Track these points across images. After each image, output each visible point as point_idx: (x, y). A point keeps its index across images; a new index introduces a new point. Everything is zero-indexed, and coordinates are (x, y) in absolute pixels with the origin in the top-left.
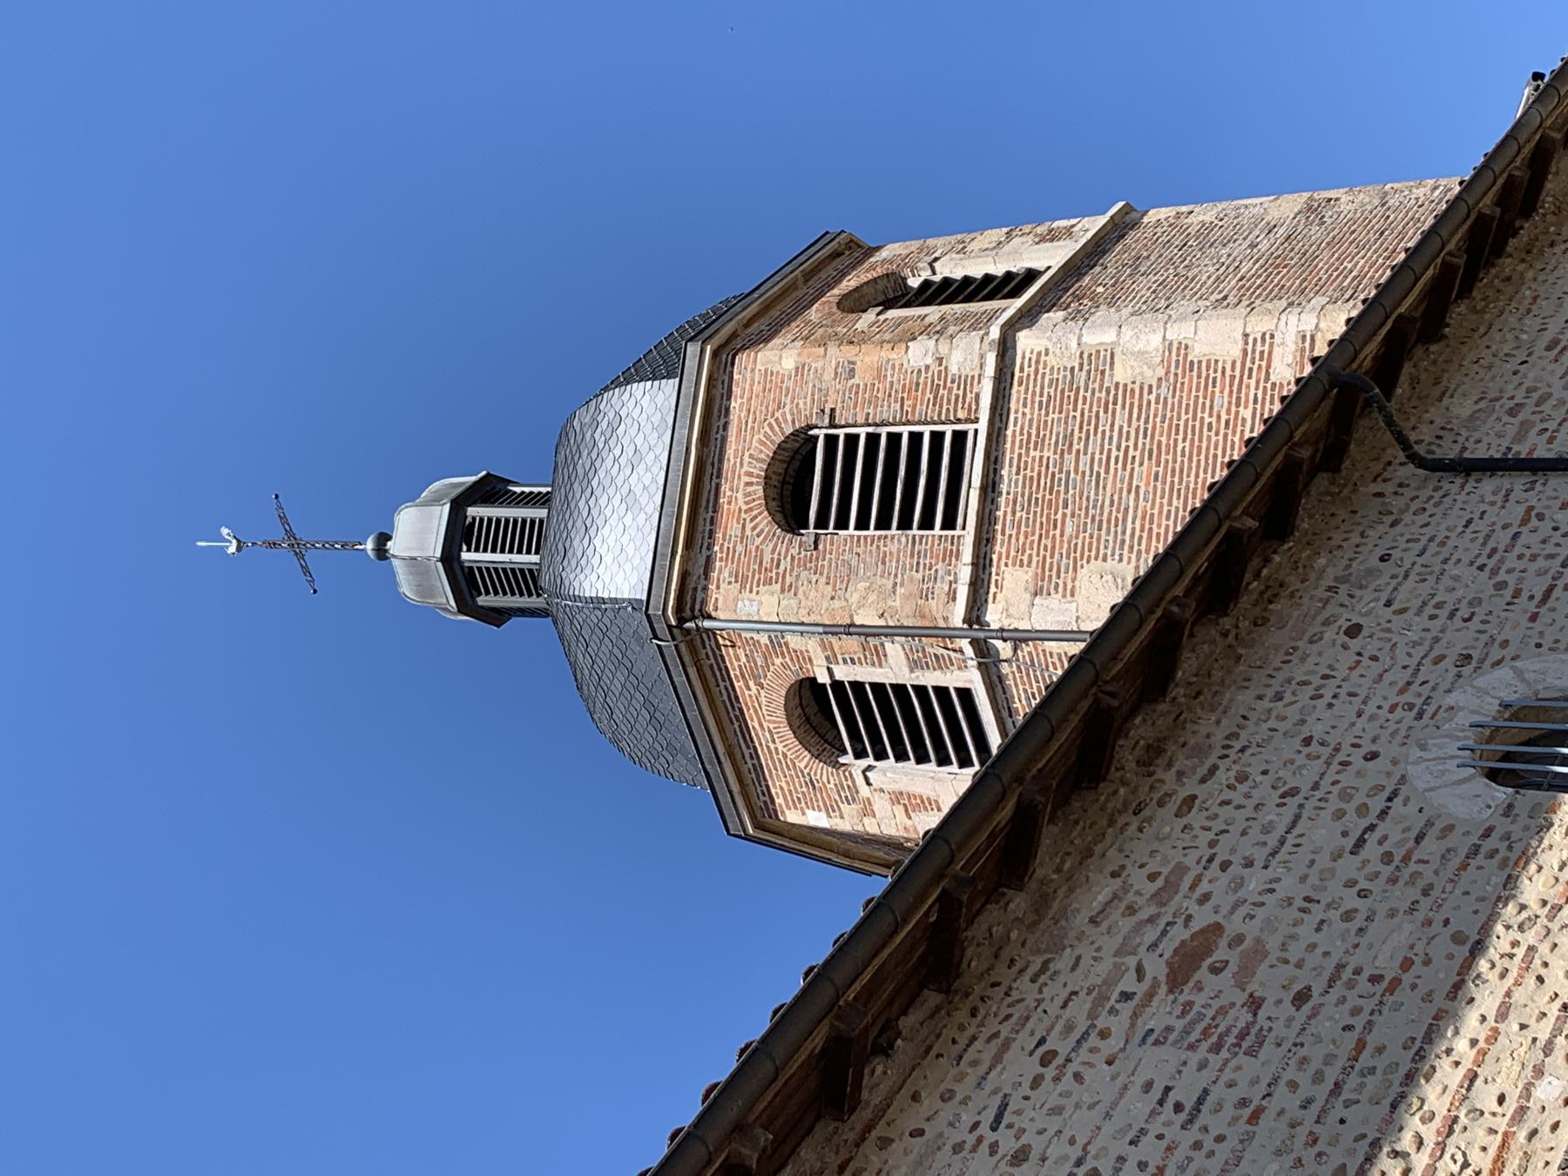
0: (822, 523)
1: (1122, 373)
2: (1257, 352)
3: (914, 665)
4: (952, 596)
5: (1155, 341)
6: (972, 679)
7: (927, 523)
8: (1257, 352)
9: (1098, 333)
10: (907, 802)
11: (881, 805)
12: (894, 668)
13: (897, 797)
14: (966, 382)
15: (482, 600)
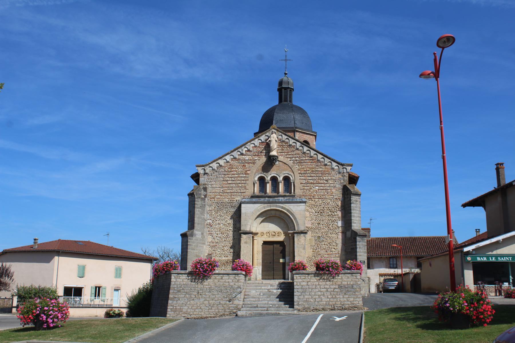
15: (283, 90)
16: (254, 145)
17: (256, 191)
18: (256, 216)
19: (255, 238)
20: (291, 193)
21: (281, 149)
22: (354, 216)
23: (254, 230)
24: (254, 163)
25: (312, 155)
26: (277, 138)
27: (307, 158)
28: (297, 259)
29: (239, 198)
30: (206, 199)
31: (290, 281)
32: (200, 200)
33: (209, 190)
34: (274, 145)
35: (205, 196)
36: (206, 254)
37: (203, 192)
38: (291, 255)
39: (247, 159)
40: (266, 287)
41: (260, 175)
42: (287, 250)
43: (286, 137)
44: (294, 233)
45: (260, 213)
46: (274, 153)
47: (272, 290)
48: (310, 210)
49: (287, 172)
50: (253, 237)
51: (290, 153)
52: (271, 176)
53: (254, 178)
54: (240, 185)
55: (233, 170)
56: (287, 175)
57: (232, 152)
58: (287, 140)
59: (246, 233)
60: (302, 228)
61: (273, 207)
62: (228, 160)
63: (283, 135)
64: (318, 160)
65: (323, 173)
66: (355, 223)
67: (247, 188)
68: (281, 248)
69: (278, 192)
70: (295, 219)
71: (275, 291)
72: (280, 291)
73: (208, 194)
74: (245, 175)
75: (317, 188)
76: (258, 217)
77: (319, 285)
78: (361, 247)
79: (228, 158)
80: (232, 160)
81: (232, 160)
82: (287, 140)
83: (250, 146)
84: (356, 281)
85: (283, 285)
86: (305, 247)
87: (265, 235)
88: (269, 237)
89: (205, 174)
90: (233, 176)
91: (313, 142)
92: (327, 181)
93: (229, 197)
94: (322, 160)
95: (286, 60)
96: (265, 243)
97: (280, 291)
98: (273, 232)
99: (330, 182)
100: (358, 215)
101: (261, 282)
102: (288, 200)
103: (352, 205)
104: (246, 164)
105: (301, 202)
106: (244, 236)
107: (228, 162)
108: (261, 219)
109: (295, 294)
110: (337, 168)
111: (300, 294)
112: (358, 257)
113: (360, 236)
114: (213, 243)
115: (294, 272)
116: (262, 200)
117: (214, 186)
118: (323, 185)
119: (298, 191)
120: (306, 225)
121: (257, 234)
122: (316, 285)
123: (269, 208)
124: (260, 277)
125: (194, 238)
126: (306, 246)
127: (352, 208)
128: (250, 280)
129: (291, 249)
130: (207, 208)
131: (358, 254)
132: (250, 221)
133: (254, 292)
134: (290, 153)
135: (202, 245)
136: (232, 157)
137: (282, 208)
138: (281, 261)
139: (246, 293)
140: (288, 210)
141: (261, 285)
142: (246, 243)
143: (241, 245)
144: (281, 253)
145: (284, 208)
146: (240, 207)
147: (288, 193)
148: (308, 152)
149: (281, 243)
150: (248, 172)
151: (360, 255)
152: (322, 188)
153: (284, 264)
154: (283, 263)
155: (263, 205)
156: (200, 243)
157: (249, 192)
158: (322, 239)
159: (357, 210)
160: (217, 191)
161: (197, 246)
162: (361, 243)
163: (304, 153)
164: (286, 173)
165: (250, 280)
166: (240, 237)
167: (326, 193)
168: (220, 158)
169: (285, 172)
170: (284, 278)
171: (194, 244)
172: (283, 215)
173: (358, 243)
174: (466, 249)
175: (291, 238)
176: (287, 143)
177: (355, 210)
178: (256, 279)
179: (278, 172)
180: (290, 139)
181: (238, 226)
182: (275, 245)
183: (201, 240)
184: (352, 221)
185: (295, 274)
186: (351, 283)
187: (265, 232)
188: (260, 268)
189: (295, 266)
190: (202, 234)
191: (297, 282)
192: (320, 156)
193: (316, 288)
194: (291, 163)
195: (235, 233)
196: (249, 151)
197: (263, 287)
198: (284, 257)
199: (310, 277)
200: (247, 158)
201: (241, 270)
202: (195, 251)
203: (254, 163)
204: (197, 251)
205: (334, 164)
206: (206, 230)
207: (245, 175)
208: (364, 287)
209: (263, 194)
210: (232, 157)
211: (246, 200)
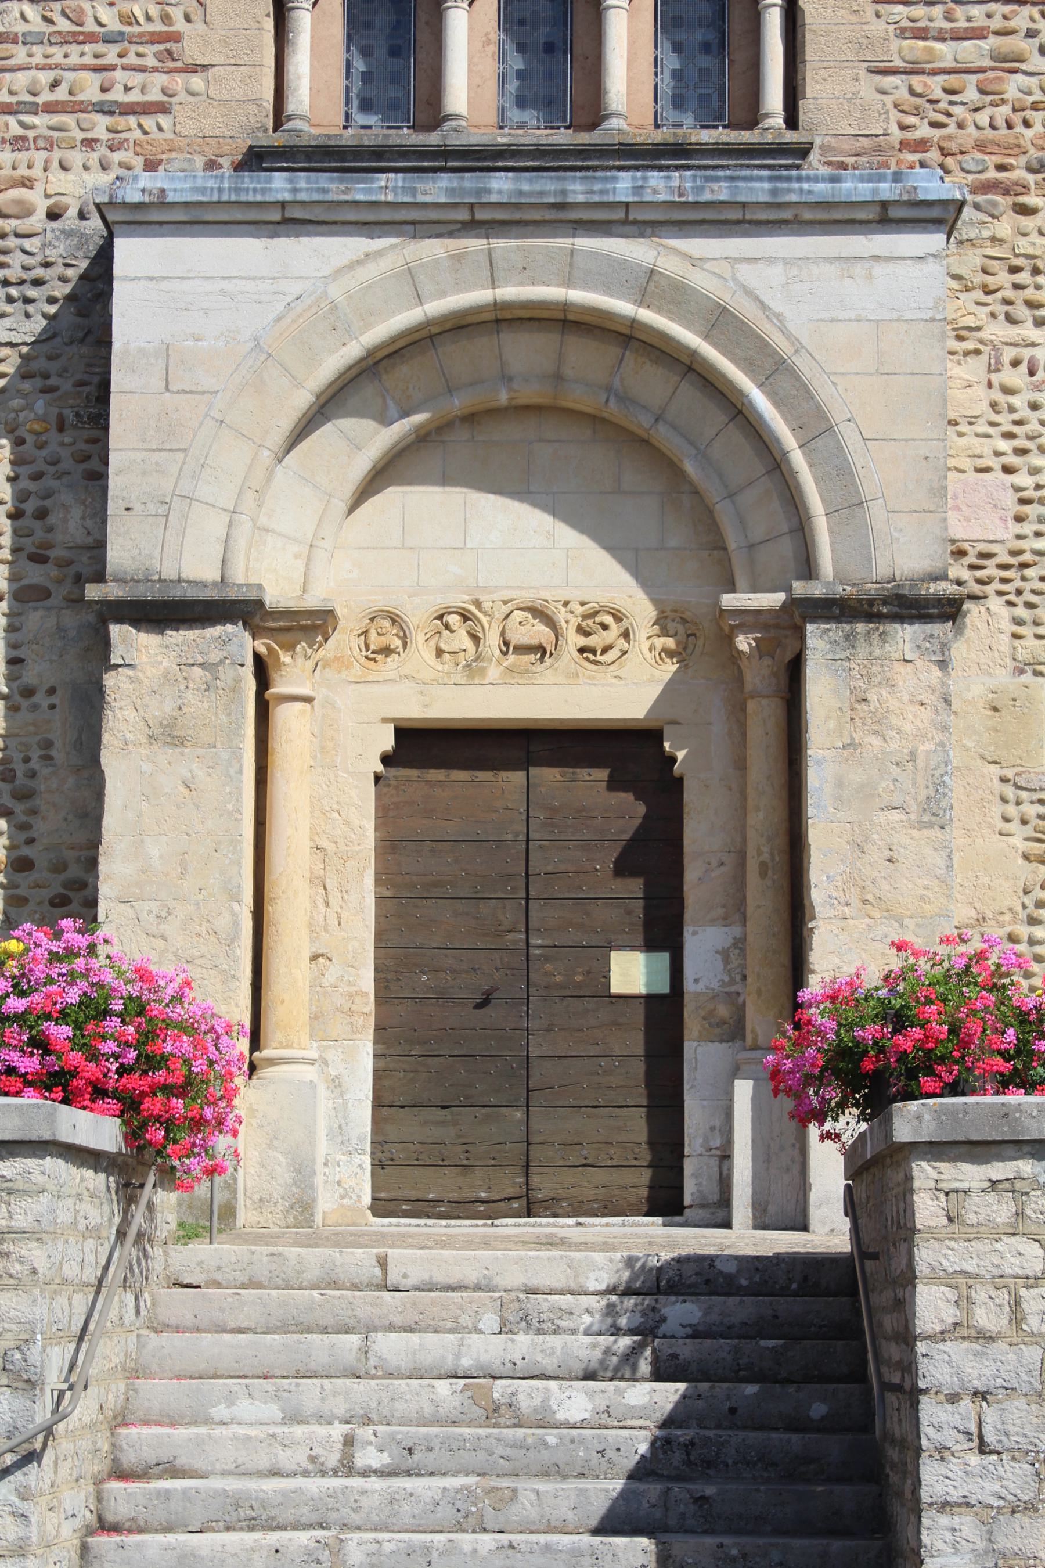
17: (301, 97)
18: (303, 399)
19: (294, 674)
20: (752, 118)
28: (846, 953)
29: (80, 183)
31: (744, 1239)
38: (762, 899)
40: (436, 1347)
42: (702, 832)
44: (803, 611)
45: (353, 351)
47: (528, 1395)
48: (997, 331)
60: (903, 554)
61: (533, 273)
67: (191, 51)
68: (627, 812)
69: (594, 114)
70: (816, 426)
71: (575, 1402)
72: (658, 1397)
76: (331, 403)
85: (681, 1312)
86: (940, 787)
87: (422, 651)
88: (473, 670)
96: (419, 746)
97: (658, 1397)
98: (526, 600)
101: (360, 1261)
105: (886, 217)
106: (142, 654)
108: (361, 441)
109: (935, 1479)
111: (1014, 1478)
115: (913, 1119)
116: (385, 187)
119: (846, 100)
120: (958, 530)
121: (313, 625)
123: (480, 296)
124: (347, 1176)
126: (956, 786)
128: (213, 1220)
129: (763, 816)
133: (253, 1410)
137: (649, 285)
138: (632, 972)
139: (141, 1442)
140: (720, 321)
141: (366, 1304)
142: (170, 735)
143: (112, 762)
144: (623, 868)
145: (674, 295)
146: (97, 281)
147: (711, 118)
149: (627, 752)
153: (664, 1012)
154: (650, 999)
155: (391, 253)
157: (222, 103)
165: (213, 1220)
166: (98, 654)
170: (666, 1202)
172: (650, 383)
175: (759, 676)
178: (302, 1208)
181: (70, 525)
182: (547, 776)
185: (937, 1150)
187: (417, 615)
188: (358, 1064)
189: (899, 1020)
191: (962, 1284)
195: (35, 619)
197: (390, 1346)
198: (663, 933)
201: (60, 1085)
209: (407, 137)
211: (179, 183)
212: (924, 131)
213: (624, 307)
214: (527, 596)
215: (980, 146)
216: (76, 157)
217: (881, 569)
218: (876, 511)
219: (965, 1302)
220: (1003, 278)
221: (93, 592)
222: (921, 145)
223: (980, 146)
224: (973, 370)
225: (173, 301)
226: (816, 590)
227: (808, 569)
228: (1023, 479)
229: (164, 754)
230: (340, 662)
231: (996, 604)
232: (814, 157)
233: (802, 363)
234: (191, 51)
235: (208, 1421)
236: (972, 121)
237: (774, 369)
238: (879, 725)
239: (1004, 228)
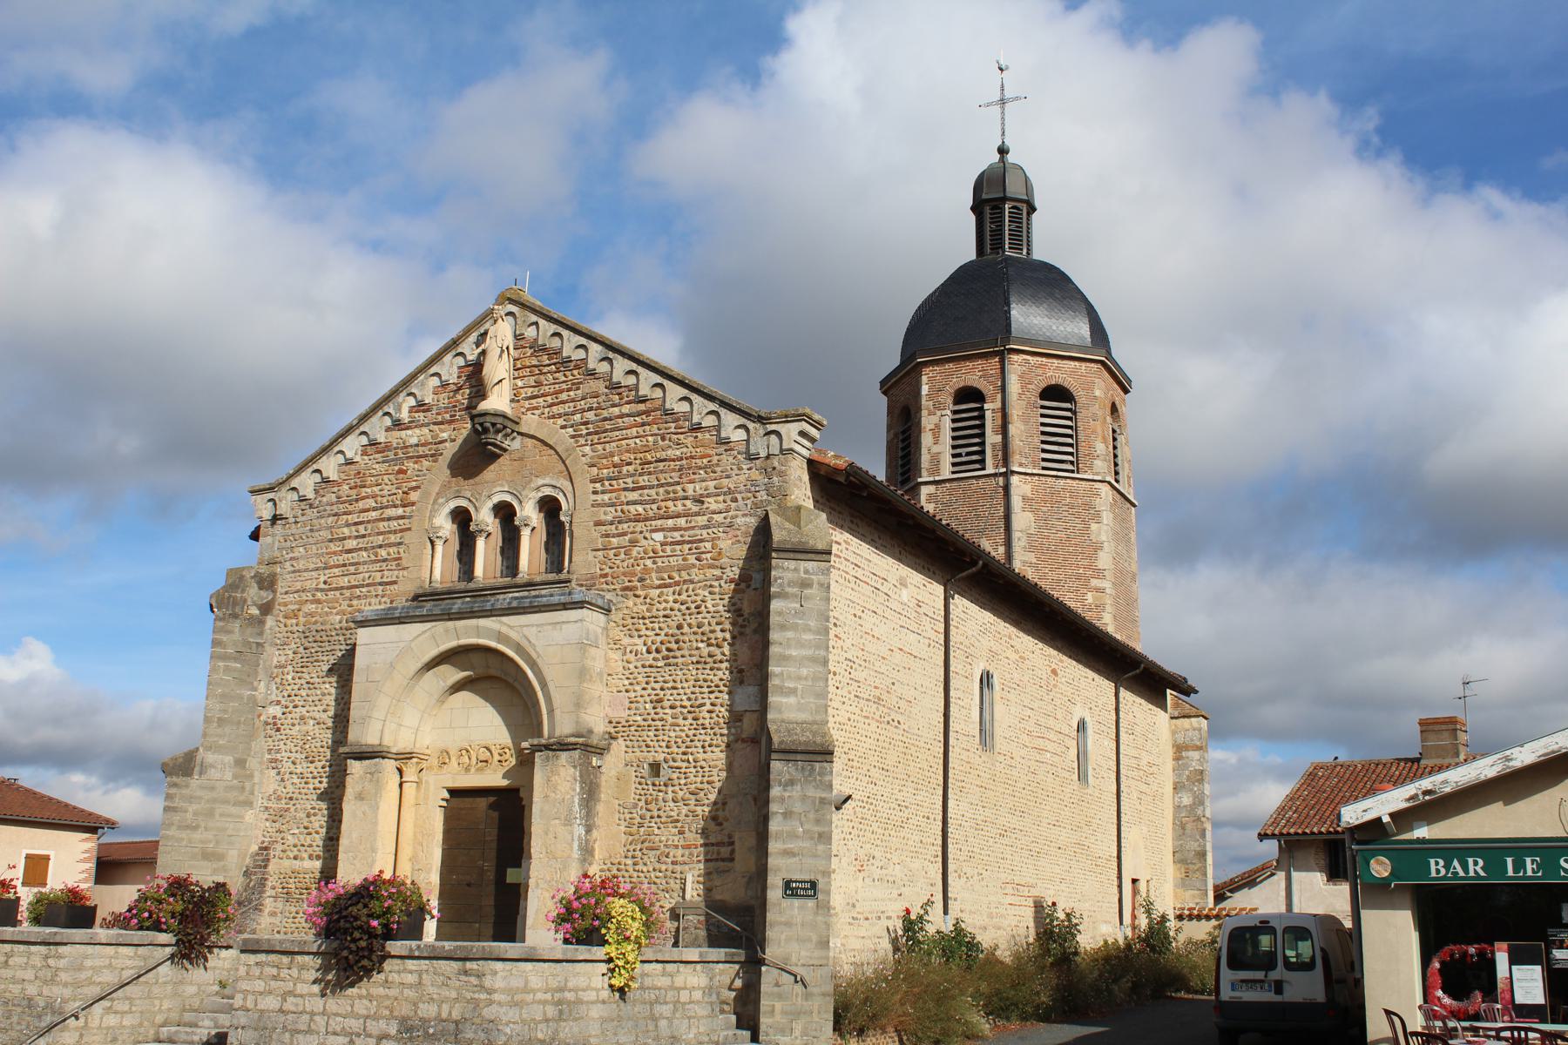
0: (1043, 407)
1: (1094, 526)
2: (1099, 574)
3: (994, 445)
4: (1021, 465)
5: (1104, 538)
6: (990, 470)
7: (1044, 451)
8: (1099, 574)
9: (1107, 517)
10: (936, 431)
11: (934, 419)
12: (993, 438)
13: (937, 426)
14: (1091, 467)
15: (987, 210)
16: (435, 381)
19: (410, 774)
21: (532, 380)
22: (785, 659)
23: (398, 741)
24: (435, 456)
25: (644, 390)
26: (518, 337)
27: (626, 409)
30: (270, 621)
32: (236, 625)
33: (281, 586)
34: (498, 369)
35: (266, 609)
36: (254, 848)
37: (253, 593)
39: (414, 441)
41: (452, 505)
43: (553, 328)
44: (537, 748)
46: (497, 401)
48: (626, 641)
49: (547, 481)
50: (400, 771)
51: (564, 396)
52: (490, 504)
53: (431, 518)
54: (383, 553)
55: (364, 492)
56: (548, 491)
57: (364, 418)
58: (556, 343)
59: (361, 756)
62: (349, 455)
63: (542, 322)
64: (668, 412)
65: (686, 468)
66: (793, 691)
70: (544, 685)
73: (280, 598)
74: (400, 511)
75: (659, 536)
77: (323, 1013)
78: (798, 807)
79: (352, 446)
80: (364, 453)
81: (364, 453)
82: (556, 343)
83: (427, 389)
84: (476, 1003)
88: (467, 770)
89: (275, 519)
90: (364, 517)
91: (1089, 387)
92: (699, 501)
93: (344, 606)
94: (685, 407)
95: (1003, 102)
99: (712, 504)
100: (810, 652)
102: (515, 604)
103: (775, 605)
104: (410, 465)
105: (565, 607)
106: (355, 767)
107: (349, 462)
110: (740, 435)
112: (772, 861)
113: (789, 753)
114: (279, 799)
117: (301, 565)
118: (682, 522)
122: (312, 1014)
125: (195, 781)
127: (774, 619)
130: (273, 656)
131: (774, 846)
132: (383, 702)
134: (564, 396)
135: (234, 810)
136: (364, 440)
137: (501, 637)
140: (519, 649)
142: (360, 797)
148: (632, 380)
150: (414, 496)
151: (788, 853)
152: (677, 535)
156: (226, 802)
158: (665, 772)
159: (807, 629)
160: (308, 585)
161: (210, 814)
162: (796, 791)
163: (614, 387)
164: (545, 485)
167: (692, 560)
168: (325, 450)
169: (540, 482)
171: (192, 808)
173: (775, 791)
174: (1353, 814)
176: (558, 352)
177: (795, 627)
179: (514, 483)
180: (565, 333)
183: (229, 788)
184: (774, 682)
186: (456, 1015)
190: (240, 763)
192: (675, 391)
193: (309, 1031)
194: (562, 437)
196: (421, 406)
199: (294, 972)
200: (412, 437)
202: (197, 836)
203: (435, 456)
204: (209, 835)
205: (730, 419)
206: (260, 744)
207: (400, 511)
208: (797, 1014)
210: (364, 440)
212: (608, 570)
213: (493, 644)
214: (483, 743)
215: (624, 574)
216: (373, 600)
217: (557, 734)
218: (557, 713)
219: (245, 999)
220: (630, 621)
221: (342, 750)
222: (606, 575)
223: (624, 574)
224: (616, 656)
225: (379, 649)
226: (543, 741)
227: (540, 735)
228: (632, 694)
229: (359, 803)
230: (430, 768)
231: (620, 741)
232: (573, 584)
233: (539, 661)
234: (404, 563)
235: (196, 1026)
236: (623, 563)
237: (533, 665)
238: (555, 789)
239: (630, 603)
